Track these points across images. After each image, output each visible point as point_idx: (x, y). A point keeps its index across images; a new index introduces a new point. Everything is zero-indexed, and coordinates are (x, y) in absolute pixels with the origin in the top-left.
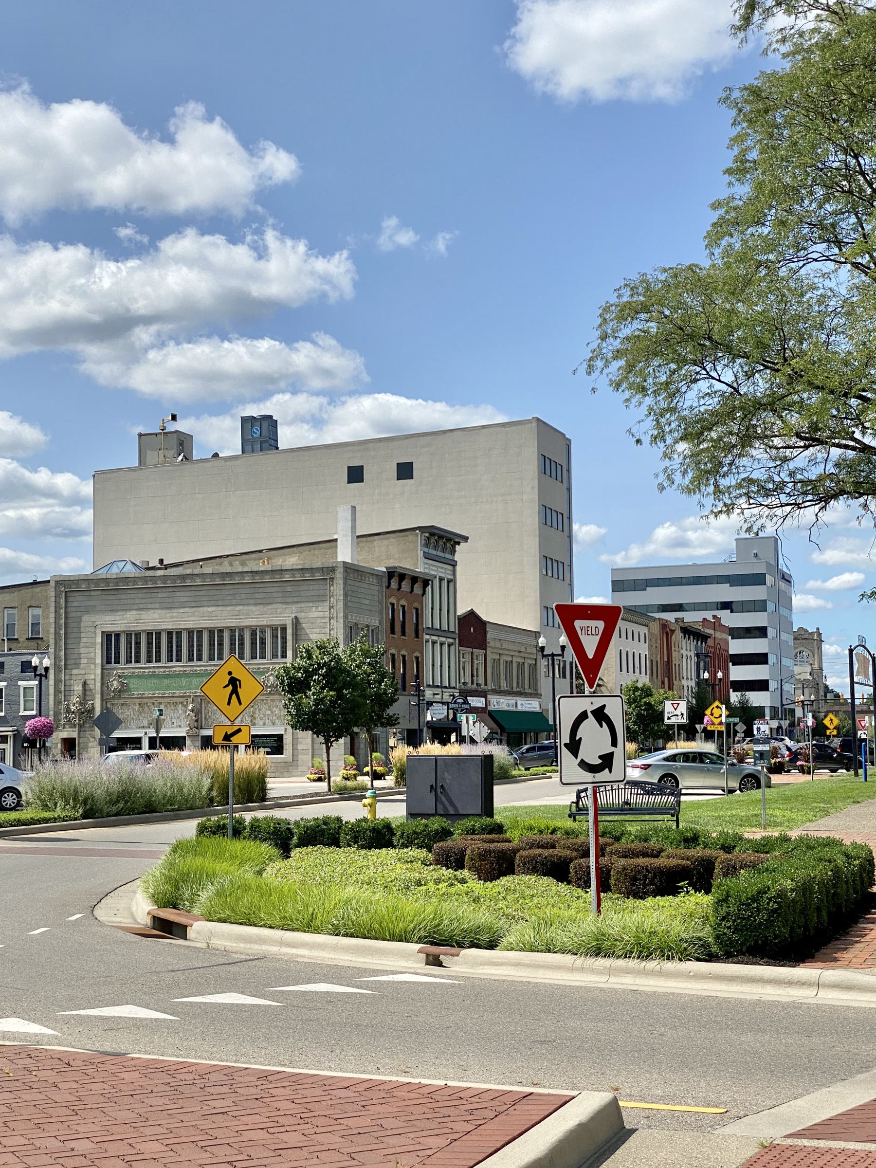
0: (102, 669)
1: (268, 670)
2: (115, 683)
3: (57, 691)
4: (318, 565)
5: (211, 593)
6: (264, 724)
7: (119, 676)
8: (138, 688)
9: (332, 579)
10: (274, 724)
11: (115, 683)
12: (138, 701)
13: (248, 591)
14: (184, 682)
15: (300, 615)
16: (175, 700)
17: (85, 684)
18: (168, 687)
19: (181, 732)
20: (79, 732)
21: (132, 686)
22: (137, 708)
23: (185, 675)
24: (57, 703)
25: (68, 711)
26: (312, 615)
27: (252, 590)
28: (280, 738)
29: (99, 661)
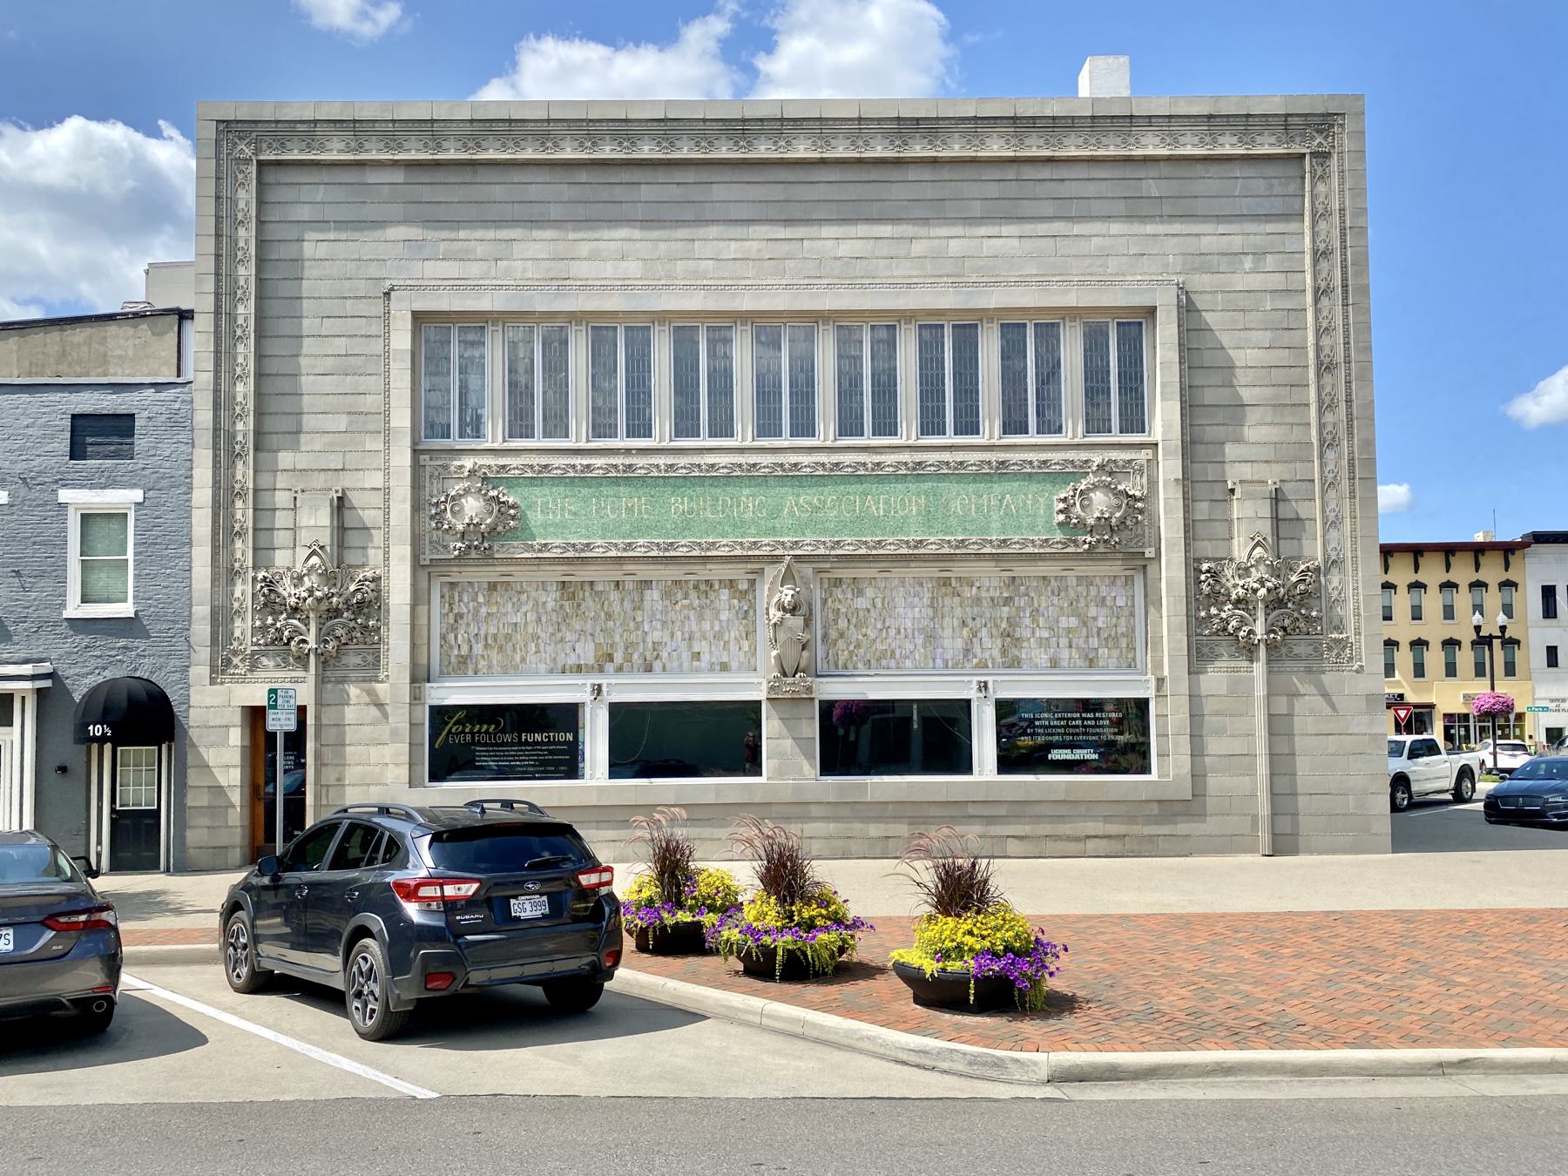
0: (416, 452)
1: (1082, 469)
2: (472, 507)
3: (224, 533)
4: (1272, 104)
5: (852, 192)
6: (1054, 663)
8: (555, 520)
9: (1322, 156)
10: (1092, 663)
12: (556, 573)
13: (992, 190)
14: (749, 501)
15: (1199, 282)
17: (341, 505)
18: (686, 527)
19: (747, 684)
20: (321, 681)
21: (535, 518)
22: (550, 599)
23: (750, 477)
24: (225, 573)
25: (270, 602)
26: (1241, 282)
27: (1011, 189)
29: (401, 419)
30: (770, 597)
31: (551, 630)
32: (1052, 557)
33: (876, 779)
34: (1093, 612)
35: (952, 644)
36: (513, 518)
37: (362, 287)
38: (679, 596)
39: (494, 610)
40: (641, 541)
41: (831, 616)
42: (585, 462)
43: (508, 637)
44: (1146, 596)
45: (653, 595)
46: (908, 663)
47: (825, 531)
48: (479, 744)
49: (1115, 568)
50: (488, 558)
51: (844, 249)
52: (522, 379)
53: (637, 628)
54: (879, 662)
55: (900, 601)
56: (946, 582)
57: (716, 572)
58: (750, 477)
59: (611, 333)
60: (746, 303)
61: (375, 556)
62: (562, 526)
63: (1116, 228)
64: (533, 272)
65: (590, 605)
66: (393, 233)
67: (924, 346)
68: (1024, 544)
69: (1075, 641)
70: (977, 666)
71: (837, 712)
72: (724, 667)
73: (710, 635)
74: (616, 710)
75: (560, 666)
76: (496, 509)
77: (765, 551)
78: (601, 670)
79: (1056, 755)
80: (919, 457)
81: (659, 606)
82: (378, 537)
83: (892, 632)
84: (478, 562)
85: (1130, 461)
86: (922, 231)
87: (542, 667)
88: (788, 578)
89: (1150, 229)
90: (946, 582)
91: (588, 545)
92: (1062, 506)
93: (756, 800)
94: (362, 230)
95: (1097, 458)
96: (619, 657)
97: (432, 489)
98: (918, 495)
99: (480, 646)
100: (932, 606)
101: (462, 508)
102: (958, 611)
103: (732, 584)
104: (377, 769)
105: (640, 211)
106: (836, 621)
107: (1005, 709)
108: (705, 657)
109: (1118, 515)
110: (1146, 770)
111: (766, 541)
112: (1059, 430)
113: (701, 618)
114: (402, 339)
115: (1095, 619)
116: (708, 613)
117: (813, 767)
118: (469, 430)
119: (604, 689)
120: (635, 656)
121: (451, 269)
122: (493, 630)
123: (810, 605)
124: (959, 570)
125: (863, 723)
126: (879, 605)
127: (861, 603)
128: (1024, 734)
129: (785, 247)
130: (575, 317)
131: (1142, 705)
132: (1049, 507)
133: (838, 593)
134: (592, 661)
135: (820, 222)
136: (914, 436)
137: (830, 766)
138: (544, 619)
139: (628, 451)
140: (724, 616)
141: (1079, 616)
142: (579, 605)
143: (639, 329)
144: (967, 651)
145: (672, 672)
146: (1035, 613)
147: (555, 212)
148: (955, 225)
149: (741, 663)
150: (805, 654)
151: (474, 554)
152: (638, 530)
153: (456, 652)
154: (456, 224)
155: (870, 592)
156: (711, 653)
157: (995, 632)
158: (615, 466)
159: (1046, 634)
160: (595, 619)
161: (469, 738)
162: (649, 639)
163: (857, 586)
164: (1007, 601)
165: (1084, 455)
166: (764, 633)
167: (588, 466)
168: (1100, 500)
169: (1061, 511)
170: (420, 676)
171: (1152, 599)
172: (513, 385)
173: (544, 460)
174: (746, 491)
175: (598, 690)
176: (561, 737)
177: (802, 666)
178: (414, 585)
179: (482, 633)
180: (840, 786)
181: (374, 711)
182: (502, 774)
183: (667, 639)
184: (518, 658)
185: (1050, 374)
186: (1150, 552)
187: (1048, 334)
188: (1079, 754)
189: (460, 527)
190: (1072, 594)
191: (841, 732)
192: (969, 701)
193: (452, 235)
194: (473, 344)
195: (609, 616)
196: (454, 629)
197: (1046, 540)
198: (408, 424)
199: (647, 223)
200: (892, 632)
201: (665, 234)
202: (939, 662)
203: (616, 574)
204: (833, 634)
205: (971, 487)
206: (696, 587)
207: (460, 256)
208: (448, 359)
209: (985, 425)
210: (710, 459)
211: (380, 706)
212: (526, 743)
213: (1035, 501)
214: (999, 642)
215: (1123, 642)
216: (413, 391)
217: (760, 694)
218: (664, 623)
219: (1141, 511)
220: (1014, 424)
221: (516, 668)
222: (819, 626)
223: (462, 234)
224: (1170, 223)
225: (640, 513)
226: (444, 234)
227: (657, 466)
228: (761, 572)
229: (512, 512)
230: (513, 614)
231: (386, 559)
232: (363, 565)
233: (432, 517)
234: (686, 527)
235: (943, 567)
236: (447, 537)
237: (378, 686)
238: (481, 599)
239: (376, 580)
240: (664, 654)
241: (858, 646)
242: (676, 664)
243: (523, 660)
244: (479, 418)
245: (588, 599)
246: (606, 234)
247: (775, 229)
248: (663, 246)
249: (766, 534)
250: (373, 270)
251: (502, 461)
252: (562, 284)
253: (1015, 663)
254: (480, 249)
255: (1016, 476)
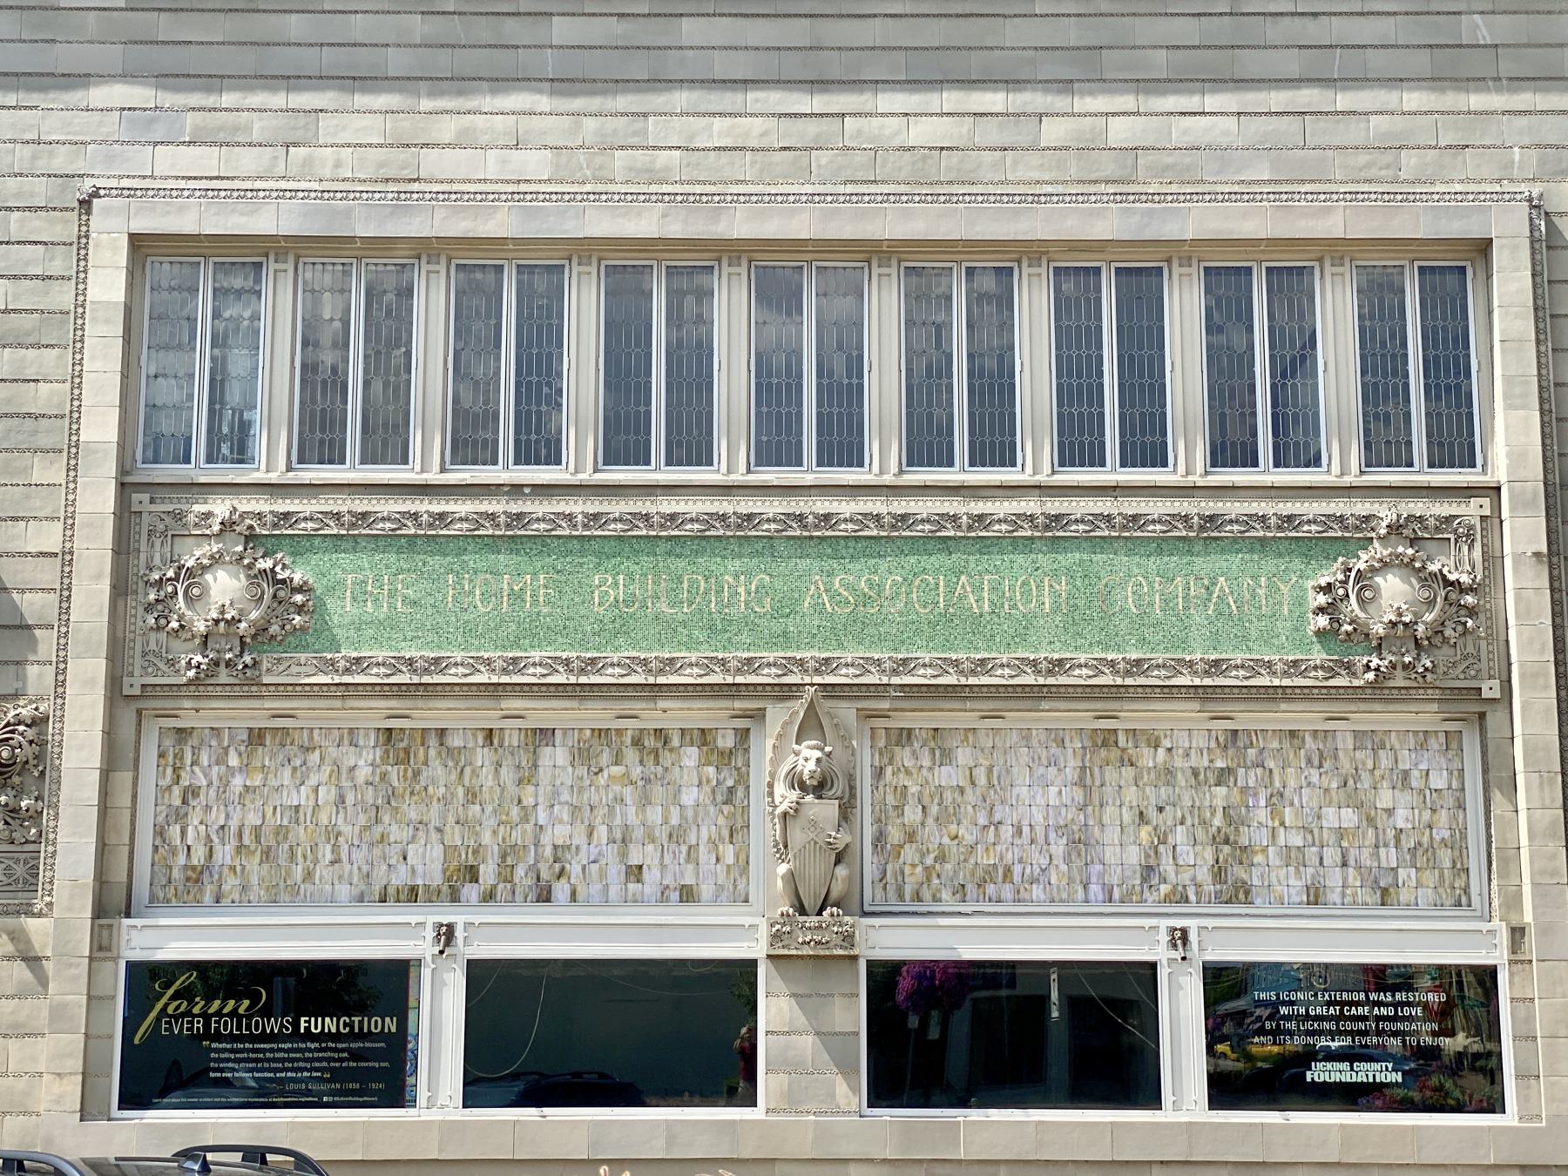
0: (122, 487)
1: (1358, 533)
2: (225, 587)
6: (1315, 896)
7: (250, 538)
10: (1386, 897)
11: (225, 587)
12: (373, 714)
14: (739, 582)
16: (653, 716)
18: (619, 626)
21: (341, 611)
22: (364, 761)
23: (739, 537)
28: (1470, 993)
29: (101, 428)
30: (776, 762)
31: (362, 819)
32: (1305, 694)
33: (975, 1115)
34: (1385, 798)
35: (1121, 853)
36: (300, 609)
37: (41, 190)
38: (605, 758)
39: (257, 780)
40: (536, 655)
41: (891, 800)
42: (437, 508)
43: (281, 832)
44: (1485, 771)
45: (555, 757)
46: (1037, 892)
47: (879, 641)
48: (218, 1037)
49: (1427, 716)
50: (250, 684)
51: (922, 133)
52: (328, 358)
53: (525, 819)
54: (985, 885)
55: (1021, 775)
56: (1107, 739)
57: (676, 715)
58: (739, 537)
59: (491, 276)
60: (740, 225)
61: (38, 677)
62: (390, 624)
63: (1413, 99)
64: (352, 165)
65: (437, 773)
66: (99, 95)
67: (1062, 306)
68: (1254, 667)
69: (1353, 854)
70: (1167, 899)
71: (905, 983)
72: (688, 895)
73: (662, 834)
74: (481, 975)
75: (377, 888)
76: (269, 592)
77: (766, 677)
78: (455, 898)
79: (1320, 1073)
80: (1055, 506)
81: (567, 776)
82: (46, 643)
83: (1007, 832)
84: (231, 693)
85: (1449, 519)
86: (1059, 102)
87: (344, 891)
88: (810, 726)
89: (1477, 101)
90: (1107, 739)
91: (437, 660)
92: (1322, 599)
93: (746, 1154)
94: (44, 89)
95: (1386, 512)
96: (488, 873)
97: (153, 558)
98: (1055, 574)
99: (229, 848)
100: (1081, 783)
101: (205, 590)
102: (1131, 794)
103: (704, 737)
104: (21, 1084)
105: (550, 63)
106: (899, 809)
107: (1223, 983)
108: (652, 876)
109: (1429, 617)
110: (1494, 1105)
111: (771, 656)
112: (1317, 462)
113: (645, 802)
114: (108, 284)
115: (1390, 812)
116: (658, 791)
117: (855, 1090)
118: (225, 450)
119: (459, 933)
120: (520, 871)
121: (206, 160)
122: (253, 819)
123: (851, 778)
124: (1132, 716)
125: (959, 1006)
126: (982, 781)
127: (947, 776)
128: (1262, 1032)
129: (812, 128)
130: (428, 249)
131: (1486, 977)
132: (1300, 601)
133: (904, 756)
134: (437, 880)
135: (877, 84)
136: (1047, 469)
137: (888, 1086)
138: (350, 799)
139: (516, 490)
140: (689, 797)
141: (1359, 806)
142: (416, 774)
143: (544, 268)
144: (1148, 871)
145: (588, 903)
146: (1277, 799)
147: (397, 63)
148: (1123, 92)
149: (720, 888)
150: (841, 871)
151: (223, 676)
152: (531, 632)
153: (181, 859)
154: (214, 81)
155: (963, 756)
156: (663, 866)
157: (1200, 834)
158: (492, 517)
159: (1297, 840)
160: (445, 801)
161: (199, 1025)
162: (546, 839)
163: (940, 745)
164: (1223, 776)
165: (1362, 508)
166: (763, 833)
167: (442, 516)
168: (1394, 591)
169: (1321, 610)
170: (112, 904)
171: (1497, 777)
172: (309, 368)
173: (361, 505)
174: (734, 565)
175: (447, 935)
176: (375, 1024)
177: (834, 895)
178: (109, 734)
179: (234, 824)
180: (907, 1127)
181: (20, 971)
182: (263, 1097)
183: (580, 839)
184: (298, 872)
185: (1295, 361)
186: (1491, 689)
187: (1292, 285)
188: (1365, 1073)
189: (201, 627)
190: (1346, 766)
191: (913, 1022)
192: (1153, 966)
193: (211, 101)
194: (239, 293)
195: (472, 796)
196: (180, 816)
197: (1295, 663)
198: (113, 436)
199: (562, 84)
200: (1007, 832)
201: (594, 103)
202: (1095, 888)
203: (487, 715)
204: (895, 835)
205: (1153, 563)
206: (637, 742)
207: (221, 137)
208: (192, 320)
209: (1177, 448)
210: (668, 505)
211: (33, 961)
212: (308, 1035)
213: (1272, 589)
214: (1209, 854)
215: (1445, 857)
216: (125, 376)
217: (755, 948)
218: (575, 809)
219: (1472, 612)
220: (1230, 447)
221: (294, 891)
222: (868, 819)
223: (228, 99)
224: (1511, 90)
225: (535, 602)
226: (196, 99)
227: (570, 517)
228: (759, 716)
229: (299, 598)
230: (295, 792)
231: (60, 684)
232: (16, 696)
233: (149, 608)
234: (619, 626)
235: (1102, 711)
236: (176, 644)
237: (31, 924)
238: (234, 761)
239: (39, 722)
240: (575, 869)
241: (942, 858)
242: (596, 888)
243: (309, 876)
244: (244, 428)
245: (435, 763)
246: (488, 102)
247: (795, 96)
248: (590, 124)
249: (771, 645)
250: (61, 161)
251: (283, 506)
252: (405, 189)
253: (1240, 894)
254: (259, 127)
255: (1235, 544)
